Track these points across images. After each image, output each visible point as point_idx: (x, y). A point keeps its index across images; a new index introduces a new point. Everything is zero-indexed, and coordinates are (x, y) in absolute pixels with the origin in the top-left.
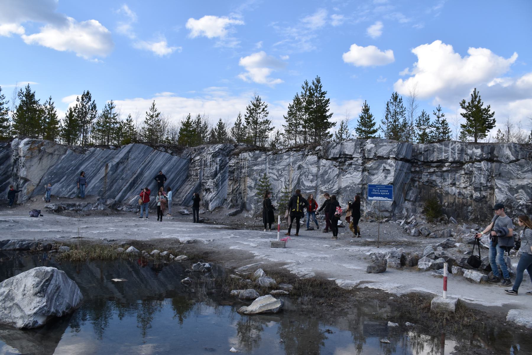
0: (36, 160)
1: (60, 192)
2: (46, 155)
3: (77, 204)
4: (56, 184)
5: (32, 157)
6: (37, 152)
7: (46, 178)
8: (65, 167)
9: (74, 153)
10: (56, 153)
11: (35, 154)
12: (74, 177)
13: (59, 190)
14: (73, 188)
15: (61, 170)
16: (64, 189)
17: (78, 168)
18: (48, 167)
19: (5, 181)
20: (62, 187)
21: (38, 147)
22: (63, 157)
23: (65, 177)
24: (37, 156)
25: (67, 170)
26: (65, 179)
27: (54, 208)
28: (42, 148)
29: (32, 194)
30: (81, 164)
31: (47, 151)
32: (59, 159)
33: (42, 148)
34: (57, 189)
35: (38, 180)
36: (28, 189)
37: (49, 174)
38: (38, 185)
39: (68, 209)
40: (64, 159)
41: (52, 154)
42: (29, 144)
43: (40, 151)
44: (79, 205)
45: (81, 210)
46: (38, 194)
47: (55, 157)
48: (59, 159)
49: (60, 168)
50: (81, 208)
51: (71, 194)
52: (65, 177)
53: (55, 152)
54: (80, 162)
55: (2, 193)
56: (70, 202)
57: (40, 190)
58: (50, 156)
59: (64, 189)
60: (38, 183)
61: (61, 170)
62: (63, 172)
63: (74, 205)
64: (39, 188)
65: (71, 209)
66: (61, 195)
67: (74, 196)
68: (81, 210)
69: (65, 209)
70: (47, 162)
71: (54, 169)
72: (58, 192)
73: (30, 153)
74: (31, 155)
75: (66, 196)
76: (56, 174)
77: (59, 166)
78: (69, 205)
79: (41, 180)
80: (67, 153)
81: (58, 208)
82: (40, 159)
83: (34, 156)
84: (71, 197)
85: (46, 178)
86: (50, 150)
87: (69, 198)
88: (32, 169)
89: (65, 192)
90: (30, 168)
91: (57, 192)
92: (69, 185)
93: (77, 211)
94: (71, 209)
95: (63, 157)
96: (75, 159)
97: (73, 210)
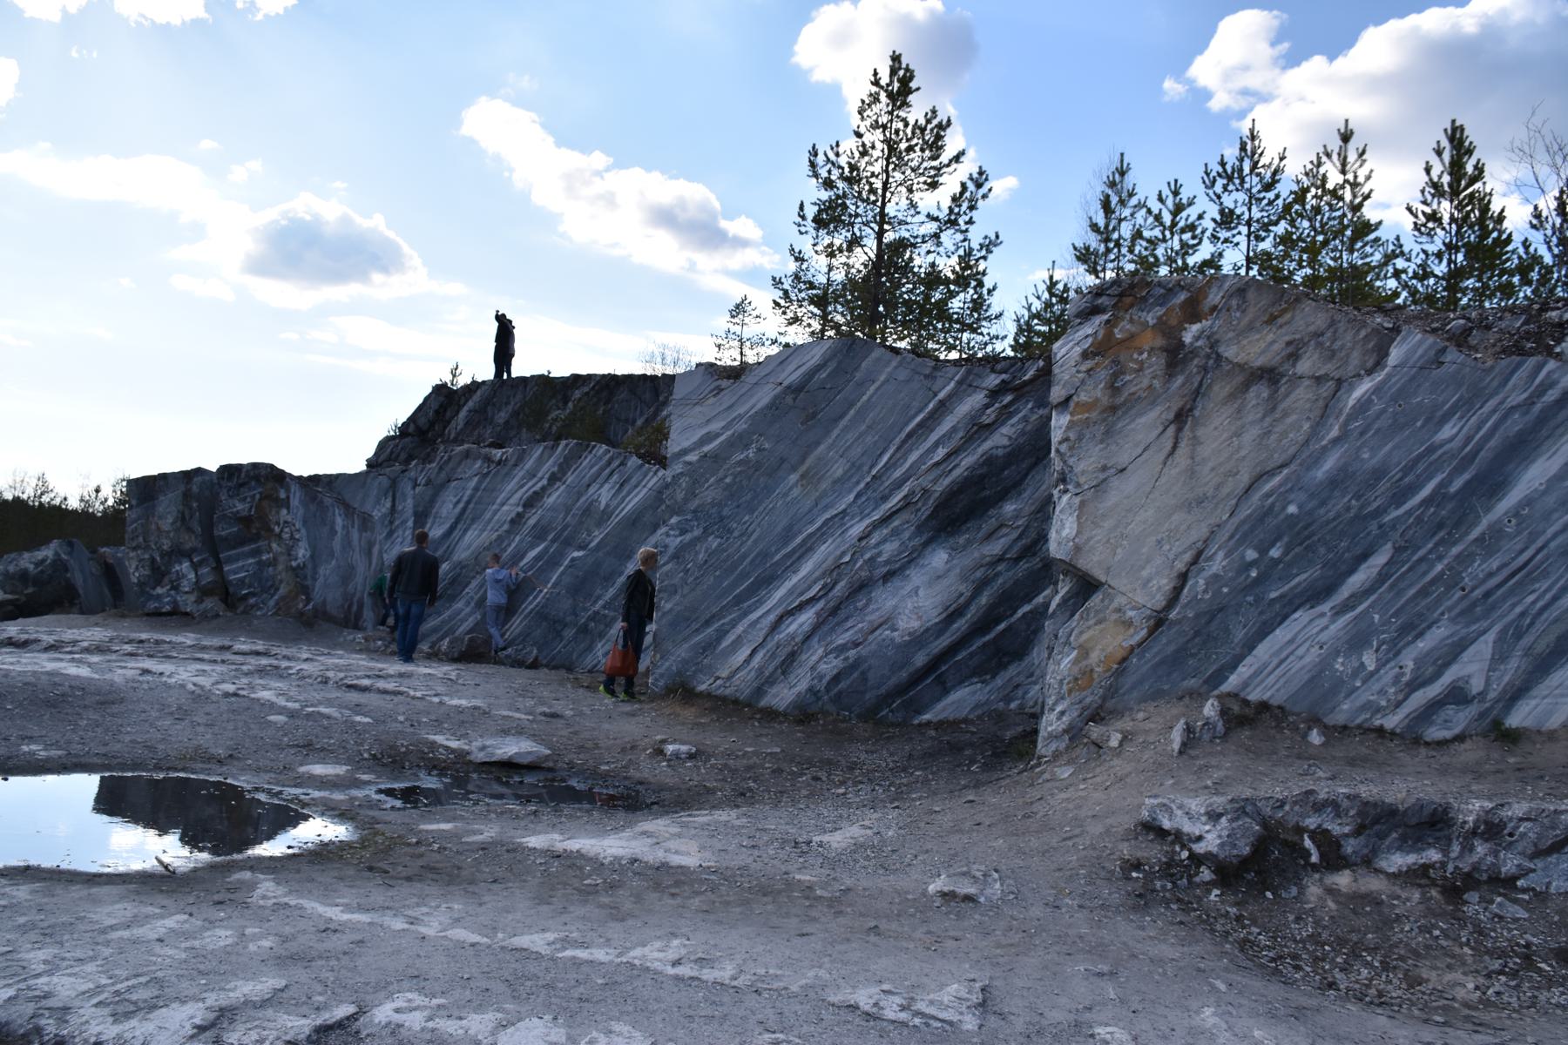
0: (1146, 425)
1: (1339, 687)
2: (1220, 390)
3: (1472, 810)
4: (1301, 616)
5: (1116, 409)
6: (1157, 363)
7: (1217, 564)
8: (1379, 474)
9: (1453, 355)
10: (1304, 366)
11: (1136, 384)
12: (1464, 559)
13: (1325, 664)
14: (1456, 650)
15: (1339, 503)
16: (1369, 660)
17: (1491, 483)
18: (1245, 478)
19: (1028, 598)
20: (1357, 641)
21: (1162, 327)
22: (1364, 387)
23: (1380, 559)
24: (1152, 397)
25: (1399, 497)
26: (1382, 577)
27: (1211, 840)
28: (1190, 334)
29: (1111, 692)
30: (1521, 448)
31: (1229, 352)
32: (1327, 409)
33: (1190, 334)
34: (1313, 655)
35: (1165, 583)
36: (1085, 652)
37: (1244, 536)
38: (1159, 621)
39: (1367, 862)
40: (1363, 406)
41: (1269, 375)
42: (1094, 311)
43: (1175, 355)
44: (1492, 829)
45: (1506, 884)
46: (1156, 695)
47: (1301, 398)
48: (1327, 409)
49: (1335, 482)
50: (1509, 864)
51: (1435, 706)
52: (1380, 559)
53: (1294, 357)
54: (1516, 424)
55: (1012, 670)
56: (1402, 788)
57: (1175, 662)
58: (1260, 391)
59: (1369, 660)
60: (1159, 601)
61: (1339, 503)
62: (1362, 518)
63: (1432, 824)
64: (1166, 643)
65: (1398, 861)
66: (1344, 711)
67: (1459, 719)
68: (1506, 884)
69: (1334, 859)
70: (1230, 439)
71: (1283, 496)
72: (1322, 686)
73: (1103, 375)
74: (1113, 389)
75: (1391, 722)
76: (1301, 534)
77: (1329, 464)
78: (1380, 822)
79: (1183, 577)
80: (1395, 354)
81: (1261, 847)
82: (1181, 418)
83: (1134, 400)
84: (1435, 733)
85: (1217, 564)
86: (1258, 348)
87: (1411, 737)
88: (1120, 491)
89: (1378, 690)
90: (1100, 487)
91: (1313, 681)
92: (1412, 629)
93: (1455, 889)
94: (1398, 861)
95: (1364, 387)
96: (1466, 405)
97: (1418, 875)
